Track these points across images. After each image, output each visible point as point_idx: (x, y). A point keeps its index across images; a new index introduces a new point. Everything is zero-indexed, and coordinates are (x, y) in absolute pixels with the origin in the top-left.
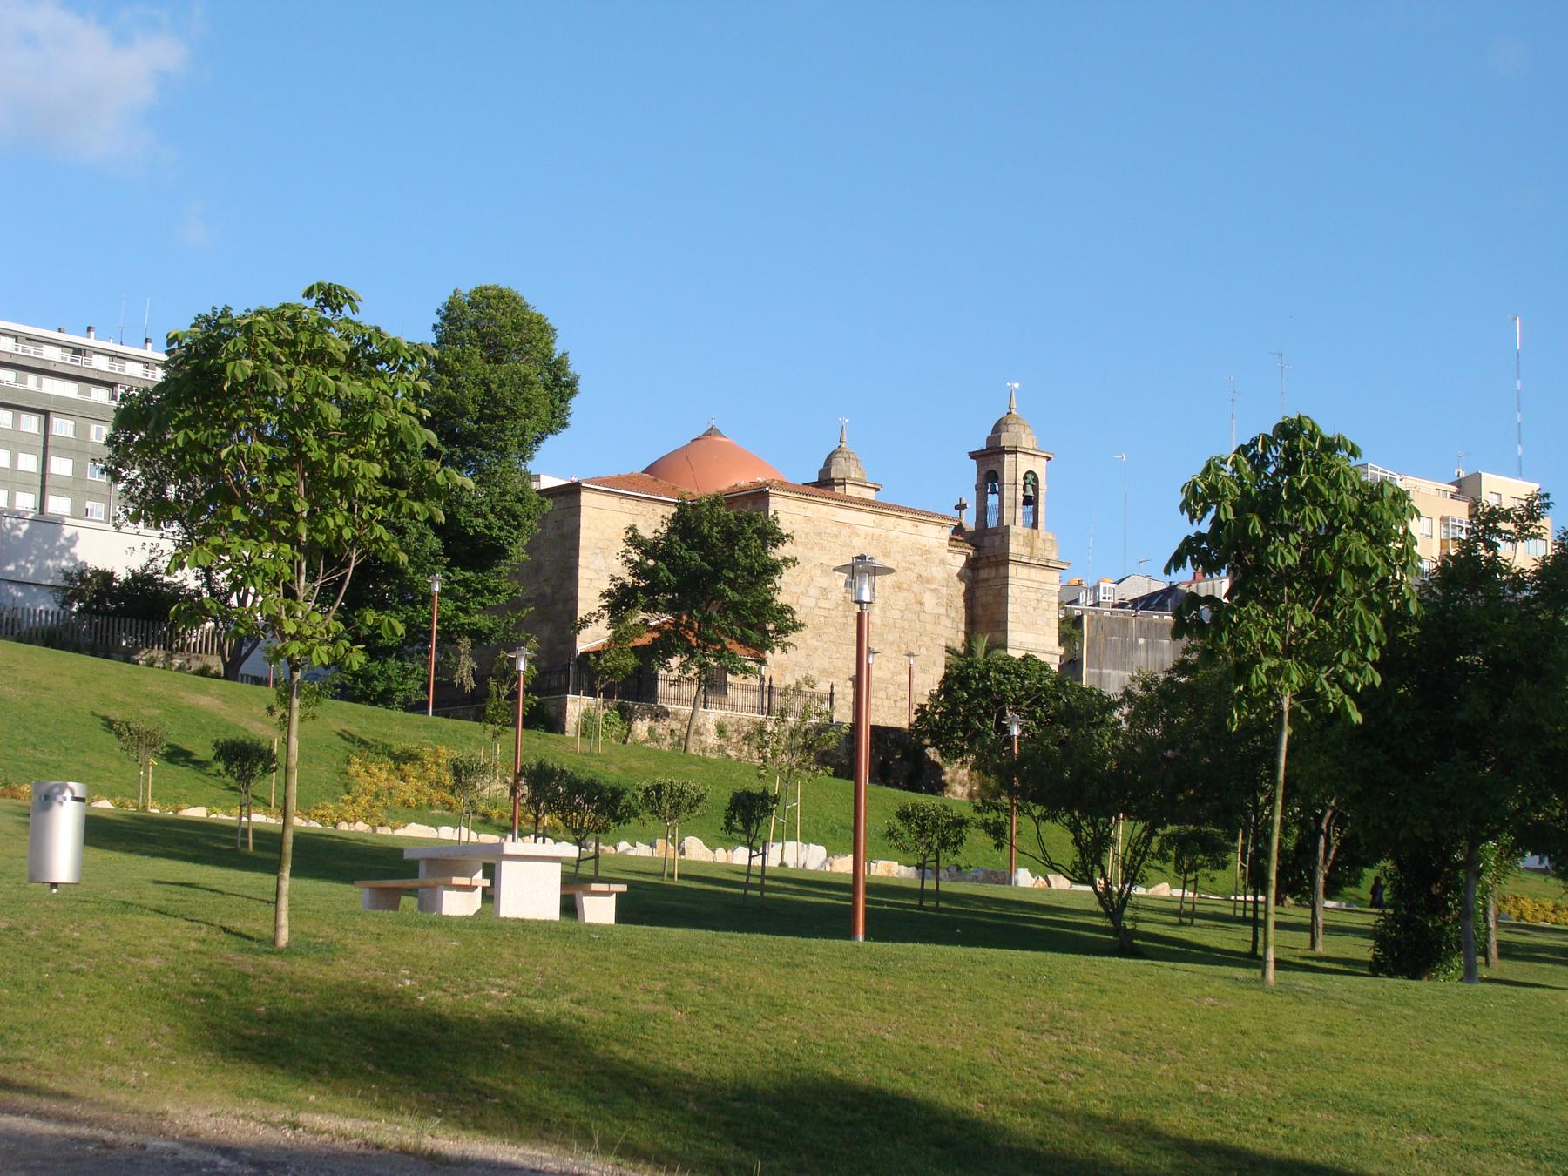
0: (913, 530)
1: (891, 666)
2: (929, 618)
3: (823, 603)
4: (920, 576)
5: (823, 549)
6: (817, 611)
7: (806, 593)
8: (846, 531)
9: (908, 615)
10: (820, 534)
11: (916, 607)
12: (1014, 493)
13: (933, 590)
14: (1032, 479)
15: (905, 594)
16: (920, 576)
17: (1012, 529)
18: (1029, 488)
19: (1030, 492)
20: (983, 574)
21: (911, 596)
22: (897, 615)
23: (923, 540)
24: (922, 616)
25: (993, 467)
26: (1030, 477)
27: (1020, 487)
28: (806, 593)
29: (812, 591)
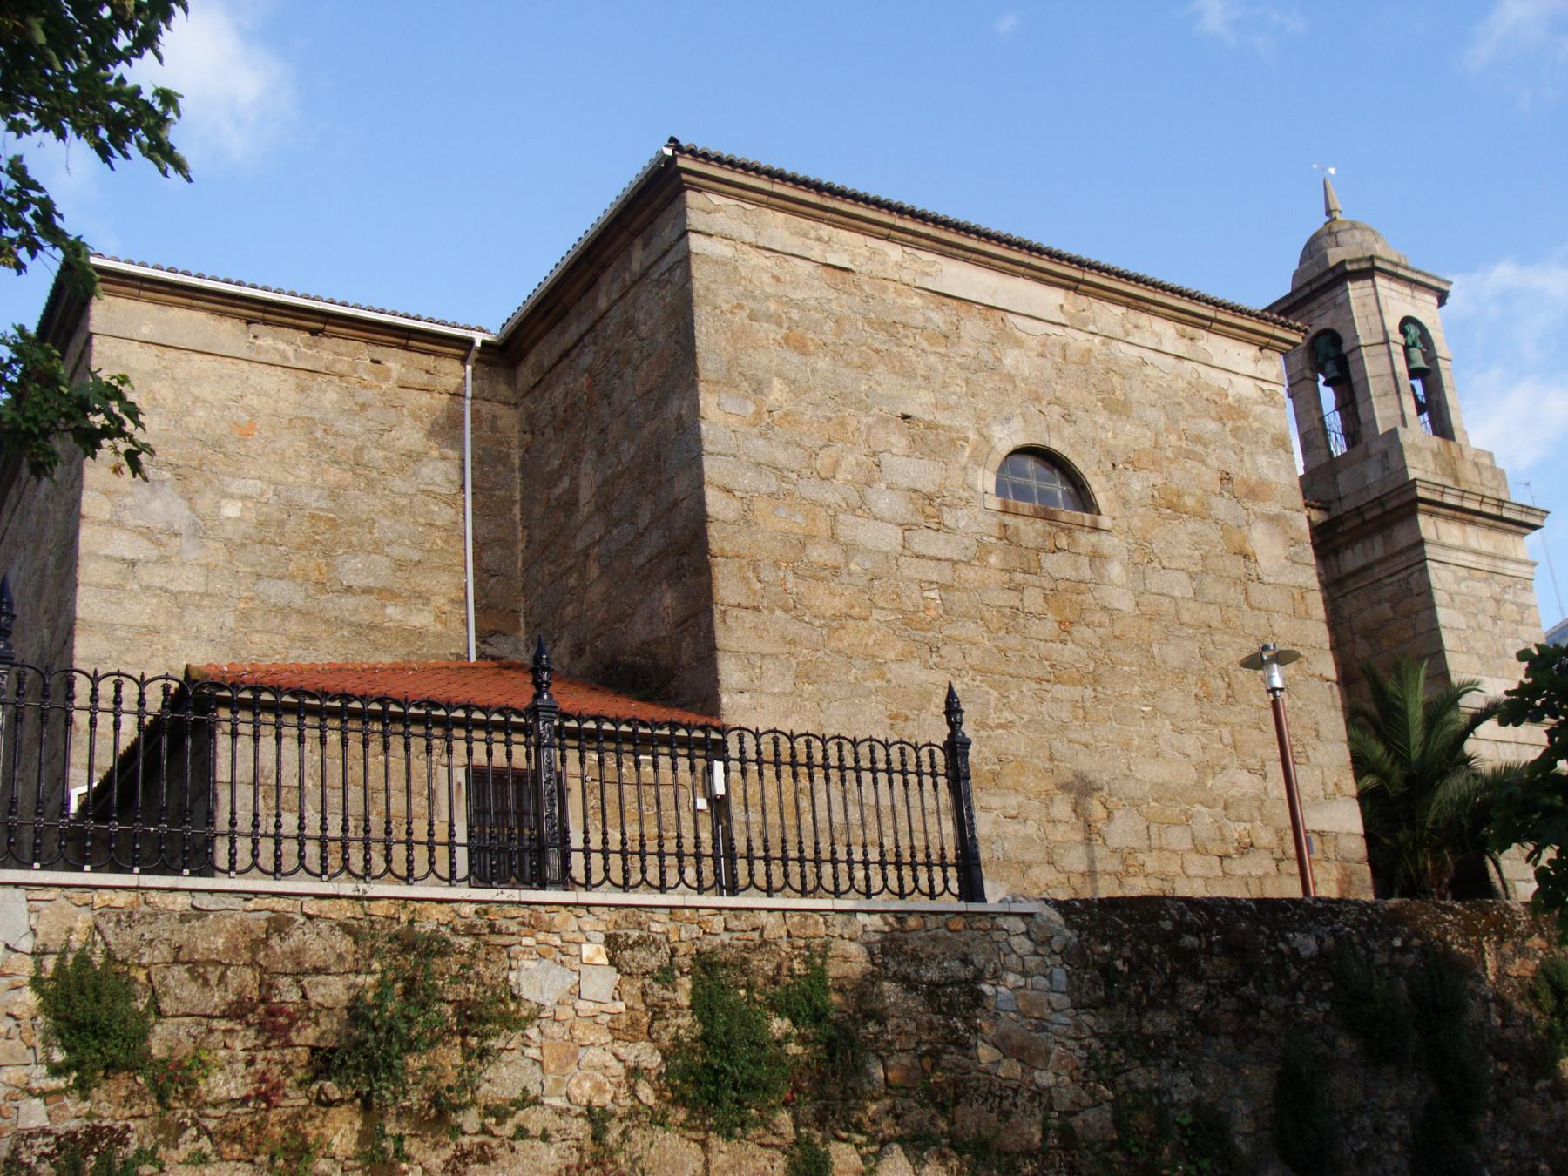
0: (1181, 348)
1: (1190, 743)
2: (1276, 599)
3: (925, 542)
4: (1226, 478)
5: (908, 373)
6: (911, 568)
7: (861, 508)
8: (974, 327)
9: (1215, 590)
10: (890, 328)
11: (1236, 567)
12: (1381, 369)
13: (1273, 520)
14: (1414, 332)
15: (1193, 526)
16: (1226, 478)
17: (1405, 437)
18: (1416, 354)
19: (1420, 363)
20: (1353, 559)
21: (1213, 534)
22: (1181, 587)
23: (1219, 379)
24: (1256, 592)
25: (1324, 323)
26: (1412, 329)
27: (1398, 350)
28: (861, 508)
29: (884, 501)
